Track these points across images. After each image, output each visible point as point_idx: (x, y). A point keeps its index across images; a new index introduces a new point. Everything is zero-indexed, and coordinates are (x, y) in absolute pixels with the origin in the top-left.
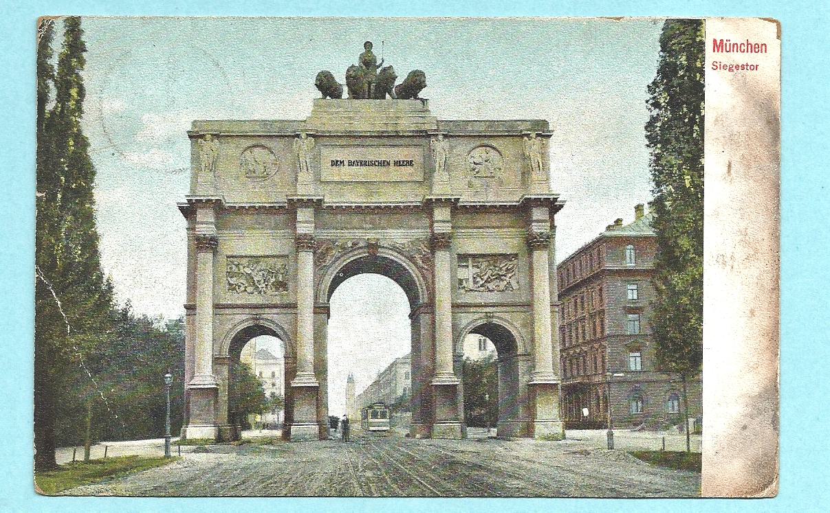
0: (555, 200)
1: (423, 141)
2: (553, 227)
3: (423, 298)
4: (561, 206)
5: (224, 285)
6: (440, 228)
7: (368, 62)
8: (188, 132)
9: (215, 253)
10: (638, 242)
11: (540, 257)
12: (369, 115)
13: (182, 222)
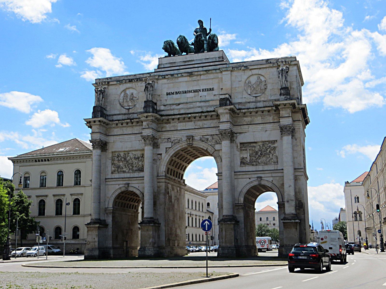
1: (220, 75)
5: (110, 168)
6: (224, 126)
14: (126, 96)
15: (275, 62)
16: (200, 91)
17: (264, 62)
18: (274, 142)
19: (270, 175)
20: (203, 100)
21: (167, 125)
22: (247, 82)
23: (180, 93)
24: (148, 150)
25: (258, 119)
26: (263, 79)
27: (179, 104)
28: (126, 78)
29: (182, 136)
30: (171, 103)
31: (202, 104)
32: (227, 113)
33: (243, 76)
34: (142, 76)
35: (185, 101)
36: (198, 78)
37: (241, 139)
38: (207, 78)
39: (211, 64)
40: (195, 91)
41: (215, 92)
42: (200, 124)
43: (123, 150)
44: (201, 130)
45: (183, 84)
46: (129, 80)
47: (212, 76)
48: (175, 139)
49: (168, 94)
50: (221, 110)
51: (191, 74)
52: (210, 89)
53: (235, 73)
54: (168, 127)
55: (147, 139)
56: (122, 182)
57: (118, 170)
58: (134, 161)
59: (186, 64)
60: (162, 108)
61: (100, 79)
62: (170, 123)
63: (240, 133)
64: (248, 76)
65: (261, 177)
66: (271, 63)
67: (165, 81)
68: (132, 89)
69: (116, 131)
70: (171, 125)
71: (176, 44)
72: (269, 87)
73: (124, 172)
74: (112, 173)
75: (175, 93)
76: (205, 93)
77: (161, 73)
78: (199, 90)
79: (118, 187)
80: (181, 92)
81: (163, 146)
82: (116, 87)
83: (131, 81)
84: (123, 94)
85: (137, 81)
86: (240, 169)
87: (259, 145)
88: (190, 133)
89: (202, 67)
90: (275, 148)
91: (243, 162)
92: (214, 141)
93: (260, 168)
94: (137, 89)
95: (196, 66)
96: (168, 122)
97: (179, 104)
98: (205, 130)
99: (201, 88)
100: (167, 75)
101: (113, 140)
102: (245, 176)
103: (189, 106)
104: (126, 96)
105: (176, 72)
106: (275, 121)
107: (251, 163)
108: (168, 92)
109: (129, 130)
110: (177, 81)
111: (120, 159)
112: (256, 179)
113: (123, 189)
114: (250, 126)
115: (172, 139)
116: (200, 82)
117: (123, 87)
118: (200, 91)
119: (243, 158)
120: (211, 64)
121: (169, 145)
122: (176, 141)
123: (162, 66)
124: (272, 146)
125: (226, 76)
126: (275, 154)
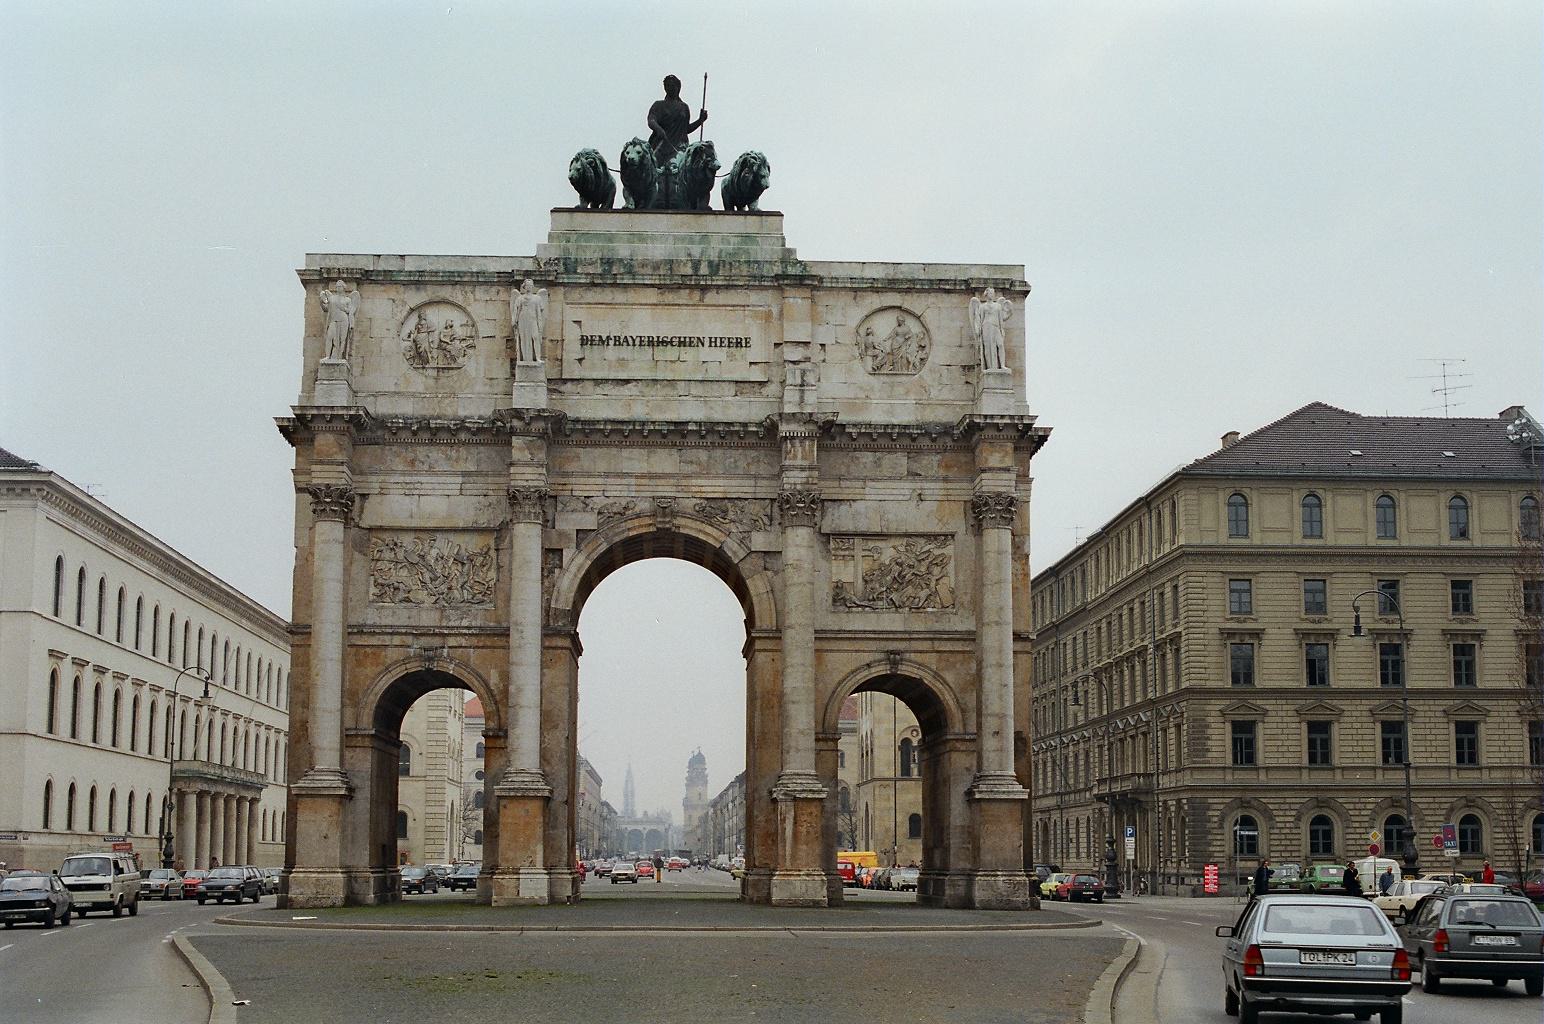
0: (1029, 426)
2: (1024, 478)
3: (765, 620)
4: (1043, 439)
6: (794, 479)
7: (671, 117)
8: (300, 273)
9: (348, 521)
10: (1023, 807)
11: (998, 539)
12: (663, 235)
13: (288, 453)
16: (703, 345)
22: (862, 331)
23: (631, 342)
25: (900, 461)
27: (627, 381)
32: (810, 438)
37: (840, 518)
43: (414, 524)
48: (611, 501)
49: (585, 341)
52: (738, 344)
55: (526, 498)
58: (455, 570)
63: (835, 500)
64: (866, 313)
68: (449, 306)
71: (614, 165)
75: (612, 342)
76: (721, 354)
78: (698, 338)
80: (634, 341)
81: (569, 522)
84: (413, 320)
86: (833, 622)
87: (894, 547)
91: (840, 597)
94: (469, 309)
97: (627, 381)
99: (706, 335)
101: (377, 485)
107: (870, 602)
111: (401, 555)
112: (882, 656)
113: (414, 667)
117: (415, 298)
118: (703, 345)
119: (839, 587)
121: (590, 521)
122: (615, 510)
124: (937, 552)
126: (945, 580)
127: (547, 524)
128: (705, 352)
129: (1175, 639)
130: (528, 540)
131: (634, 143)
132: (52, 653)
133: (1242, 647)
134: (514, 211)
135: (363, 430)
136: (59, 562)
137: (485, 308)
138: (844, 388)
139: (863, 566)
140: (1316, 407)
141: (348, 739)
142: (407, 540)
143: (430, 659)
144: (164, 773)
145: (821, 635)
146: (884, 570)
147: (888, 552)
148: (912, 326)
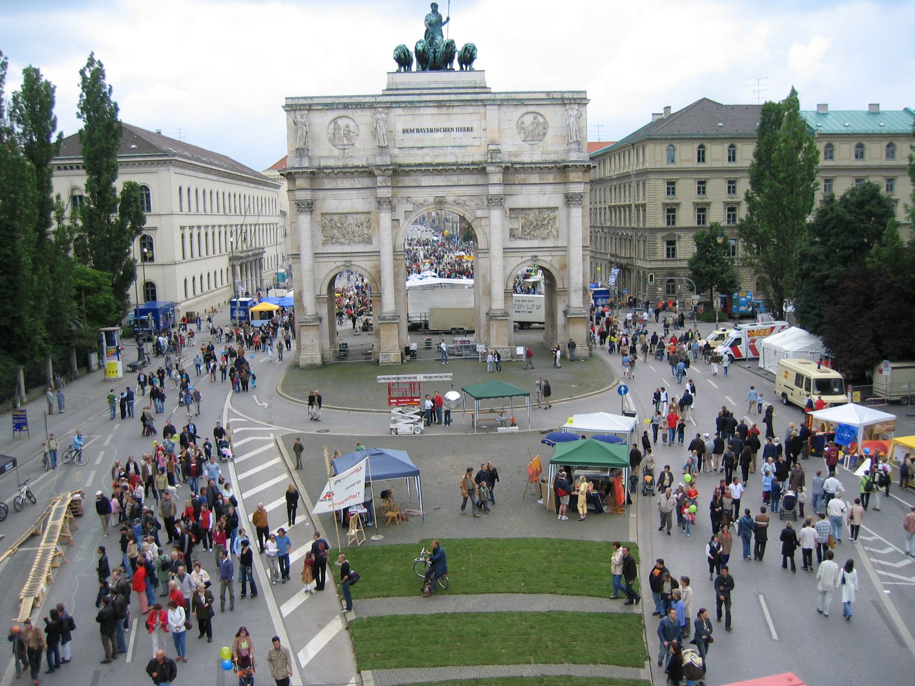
1: (482, 109)
5: (320, 238)
6: (494, 190)
9: (311, 212)
14: (337, 128)
15: (559, 96)
17: (544, 96)
18: (556, 209)
19: (548, 253)
20: (458, 144)
21: (406, 178)
24: (385, 218)
25: (534, 178)
26: (541, 120)
27: (422, 148)
28: (336, 101)
29: (428, 196)
30: (410, 145)
31: (456, 150)
33: (514, 114)
34: (363, 100)
35: (432, 145)
36: (451, 110)
38: (464, 112)
39: (469, 91)
40: (445, 130)
41: (474, 134)
42: (454, 179)
43: (339, 211)
44: (455, 189)
45: (428, 118)
46: (344, 104)
47: (470, 109)
49: (405, 131)
50: (490, 169)
51: (440, 104)
52: (468, 130)
53: (504, 109)
54: (407, 181)
56: (340, 259)
57: (330, 239)
59: (432, 86)
60: (397, 151)
61: (292, 98)
62: (409, 175)
65: (536, 257)
66: (553, 98)
67: (399, 111)
69: (328, 183)
70: (411, 178)
72: (551, 132)
73: (342, 244)
74: (325, 243)
76: (460, 134)
77: (393, 99)
79: (333, 265)
82: (322, 113)
83: (346, 106)
85: (356, 108)
88: (440, 193)
89: (456, 94)
90: (555, 218)
91: (513, 235)
92: (473, 204)
93: (535, 243)
95: (447, 91)
96: (407, 173)
97: (422, 148)
98: (462, 189)
99: (455, 125)
100: (404, 102)
102: (516, 254)
103: (438, 152)
104: (337, 128)
105: (416, 98)
106: (557, 181)
108: (406, 128)
109: (347, 183)
110: (417, 111)
114: (524, 187)
115: (413, 200)
116: (452, 116)
120: (469, 91)
121: (410, 207)
123: (395, 87)
125: (492, 111)
127: (393, 209)
128: (454, 134)
129: (644, 206)
130: (385, 218)
131: (420, 42)
132: (182, 228)
133: (671, 211)
134: (373, 74)
135: (316, 175)
136: (180, 188)
137: (363, 118)
138: (514, 147)
139: (521, 221)
140: (705, 100)
141: (318, 299)
142: (336, 218)
143: (347, 266)
144: (226, 259)
145: (506, 250)
146: (531, 223)
147: (532, 216)
148: (541, 120)
